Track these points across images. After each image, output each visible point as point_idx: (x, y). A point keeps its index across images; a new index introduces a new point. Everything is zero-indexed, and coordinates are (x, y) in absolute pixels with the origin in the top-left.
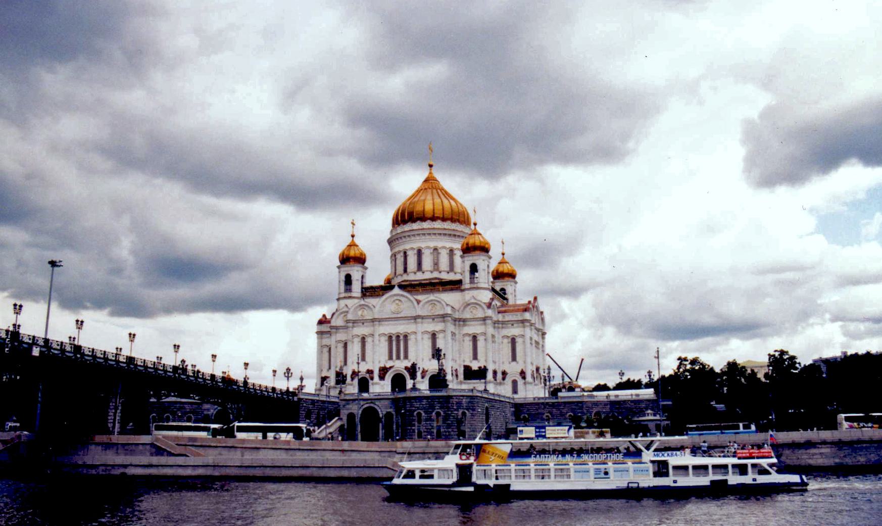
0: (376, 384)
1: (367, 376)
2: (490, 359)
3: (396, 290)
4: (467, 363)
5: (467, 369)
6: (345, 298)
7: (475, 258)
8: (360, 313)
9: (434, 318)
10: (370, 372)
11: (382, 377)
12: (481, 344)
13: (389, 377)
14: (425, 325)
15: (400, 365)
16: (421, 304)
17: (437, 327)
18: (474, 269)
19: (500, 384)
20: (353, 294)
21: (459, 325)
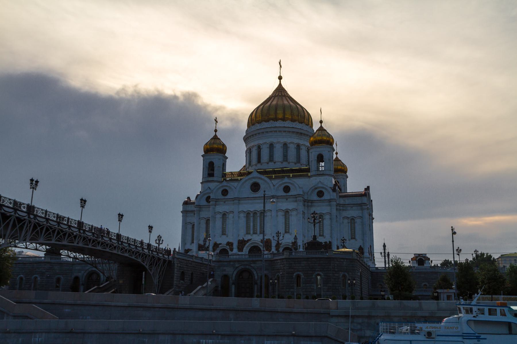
1: (228, 247)
15: (257, 239)
21: (308, 206)
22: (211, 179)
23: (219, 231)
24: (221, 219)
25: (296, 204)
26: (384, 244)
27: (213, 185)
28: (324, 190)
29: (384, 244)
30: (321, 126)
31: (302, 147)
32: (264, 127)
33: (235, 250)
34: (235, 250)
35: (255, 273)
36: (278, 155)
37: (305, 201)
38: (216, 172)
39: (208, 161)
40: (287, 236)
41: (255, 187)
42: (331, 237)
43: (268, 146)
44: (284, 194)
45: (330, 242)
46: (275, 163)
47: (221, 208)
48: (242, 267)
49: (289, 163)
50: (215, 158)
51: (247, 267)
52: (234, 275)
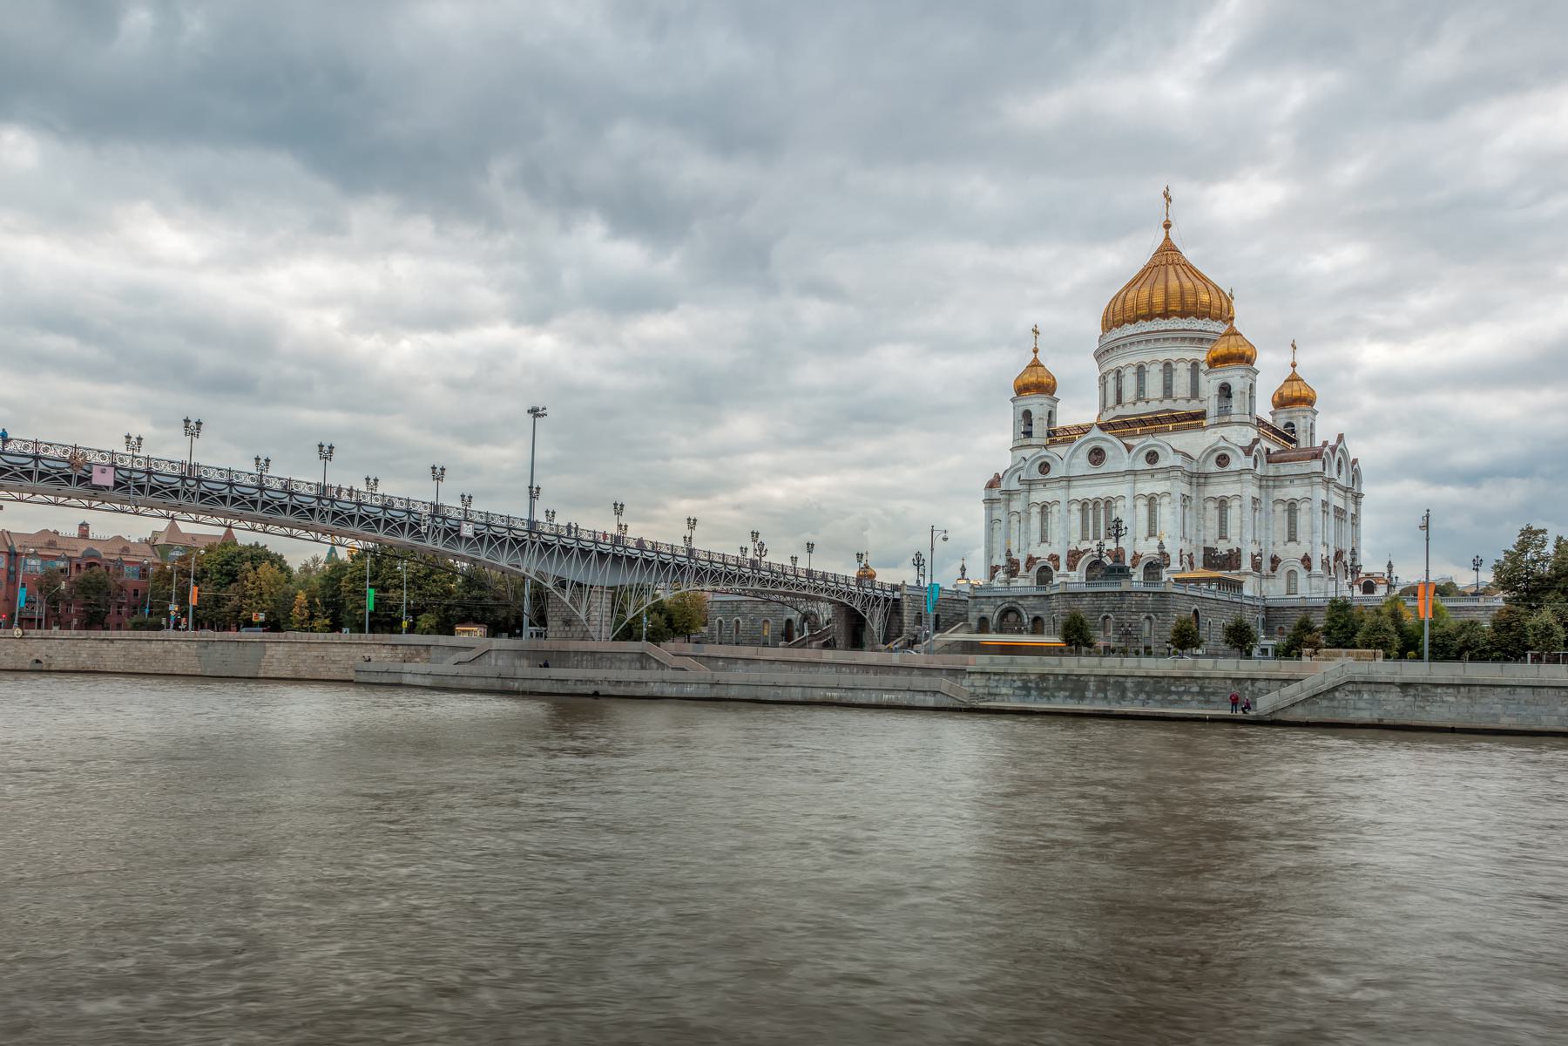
1: (1051, 565)
4: (1210, 544)
5: (1209, 552)
10: (1054, 558)
12: (1233, 513)
13: (1083, 564)
14: (1139, 485)
16: (1134, 451)
18: (1225, 391)
19: (1268, 577)
21: (1198, 485)
22: (1027, 441)
23: (1036, 536)
27: (1028, 453)
28: (1228, 453)
33: (1063, 568)
34: (1063, 568)
37: (1192, 475)
38: (1034, 429)
39: (1022, 409)
41: (1097, 455)
43: (1134, 370)
44: (1148, 466)
47: (1040, 496)
50: (1037, 404)
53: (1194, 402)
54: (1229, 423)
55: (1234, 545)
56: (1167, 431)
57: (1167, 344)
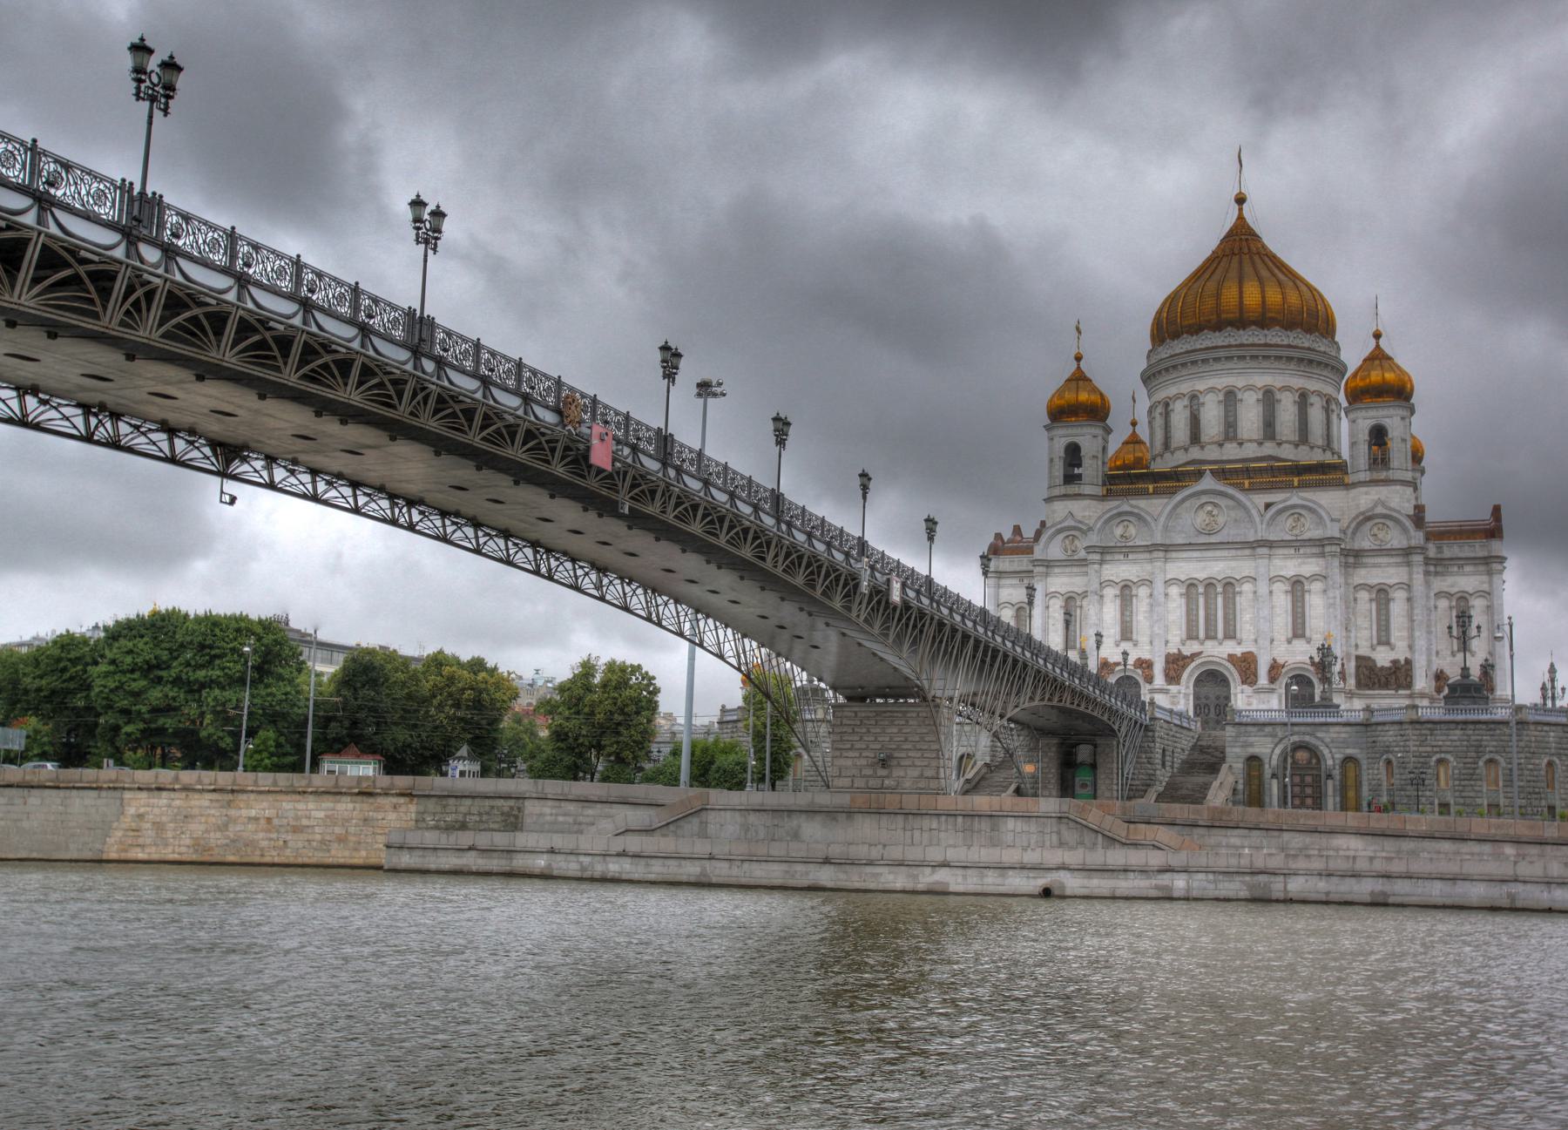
0: (1161, 691)
1: (1138, 675)
2: (1421, 643)
3: (1208, 482)
4: (1364, 651)
6: (1066, 496)
7: (1381, 413)
8: (1119, 531)
9: (1297, 544)
10: (1145, 665)
11: (1173, 677)
12: (1398, 608)
15: (1218, 651)
17: (1310, 567)
18: (1379, 435)
20: (1087, 490)
22: (1072, 489)
24: (1118, 601)
25: (1321, 561)
26: (1552, 665)
29: (1552, 665)
30: (1378, 346)
31: (1313, 399)
32: (1208, 343)
35: (1326, 752)
36: (1250, 418)
39: (1064, 442)
40: (1299, 644)
42: (1411, 647)
43: (1221, 397)
45: (1408, 662)
46: (1241, 444)
48: (1295, 738)
49: (1279, 444)
51: (1307, 738)
52: (1275, 757)
53: (1304, 449)
54: (1387, 482)
55: (1401, 654)
56: (1290, 486)
57: (1265, 364)
